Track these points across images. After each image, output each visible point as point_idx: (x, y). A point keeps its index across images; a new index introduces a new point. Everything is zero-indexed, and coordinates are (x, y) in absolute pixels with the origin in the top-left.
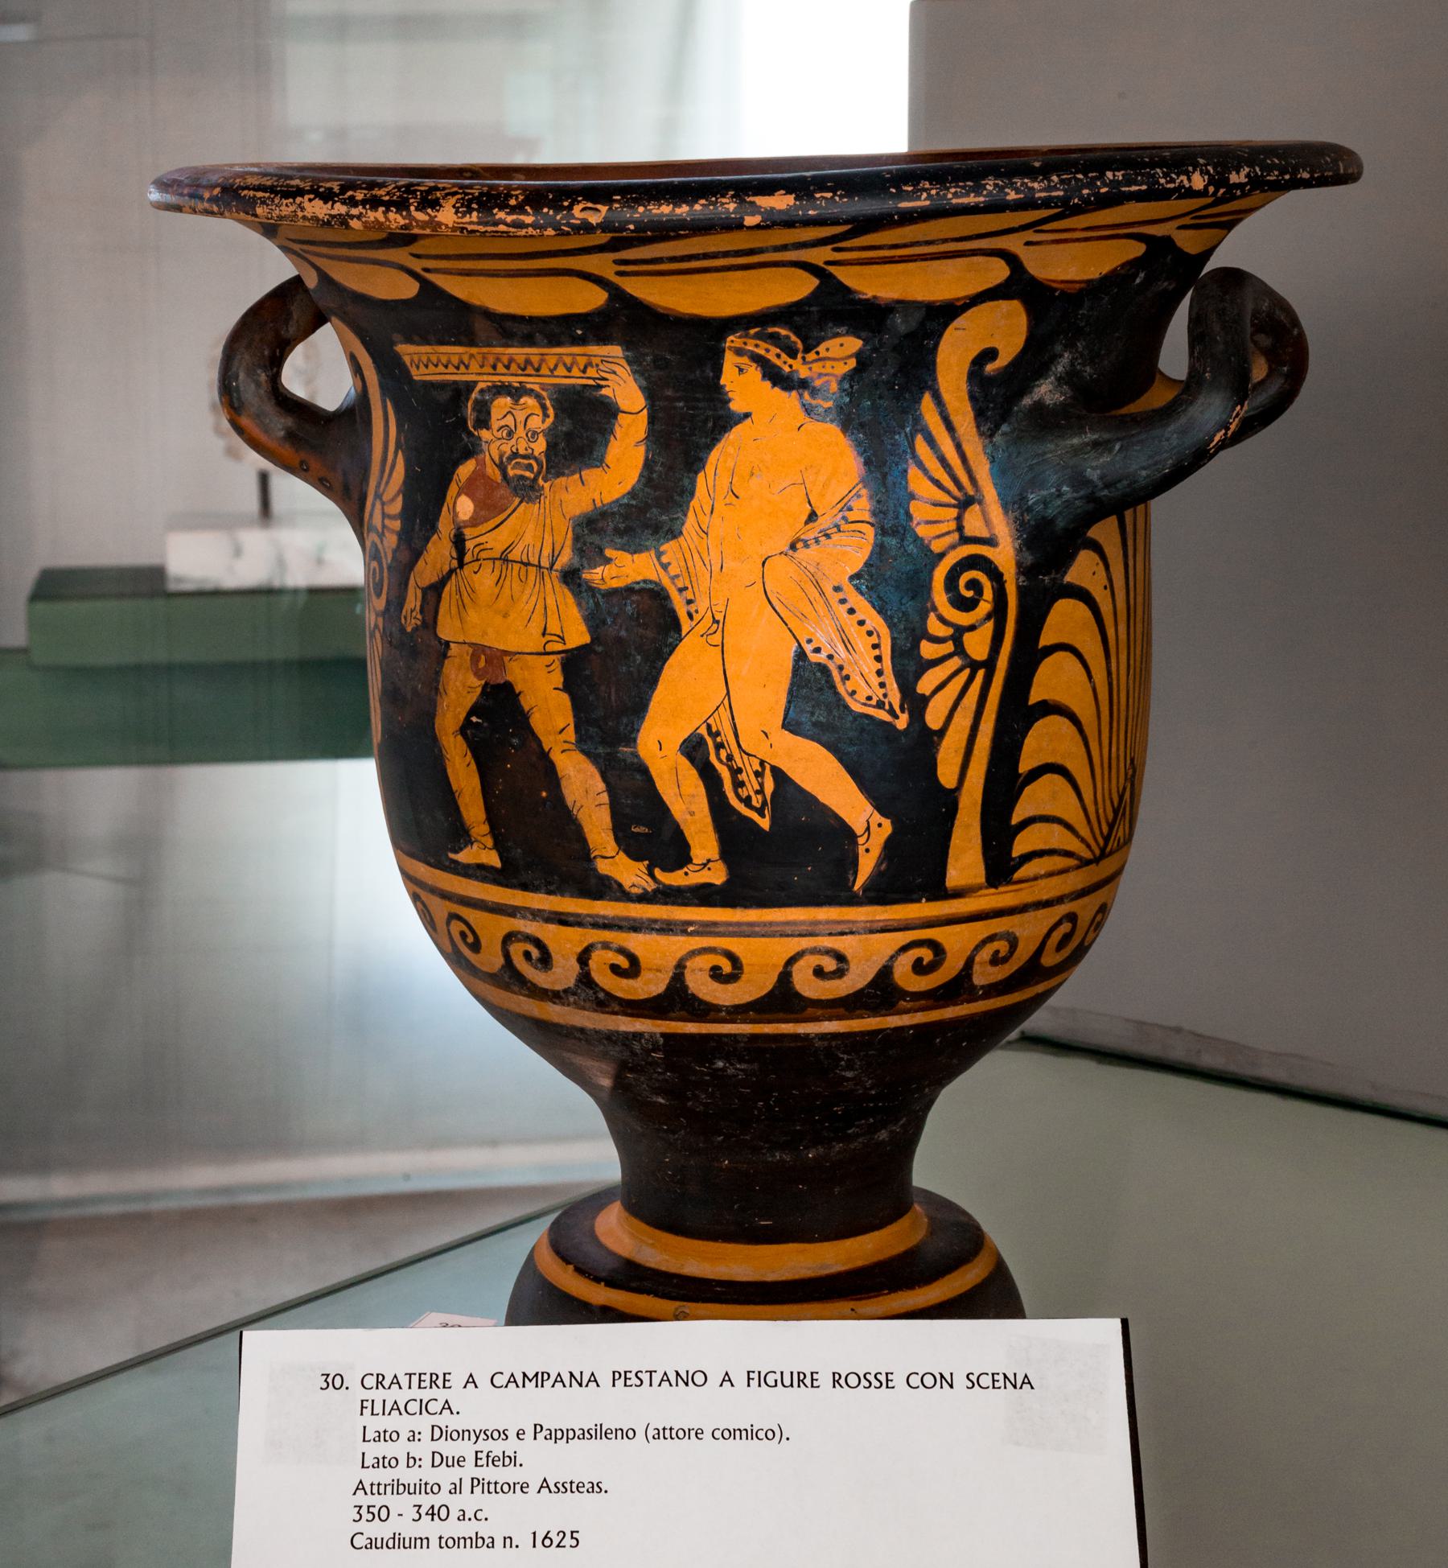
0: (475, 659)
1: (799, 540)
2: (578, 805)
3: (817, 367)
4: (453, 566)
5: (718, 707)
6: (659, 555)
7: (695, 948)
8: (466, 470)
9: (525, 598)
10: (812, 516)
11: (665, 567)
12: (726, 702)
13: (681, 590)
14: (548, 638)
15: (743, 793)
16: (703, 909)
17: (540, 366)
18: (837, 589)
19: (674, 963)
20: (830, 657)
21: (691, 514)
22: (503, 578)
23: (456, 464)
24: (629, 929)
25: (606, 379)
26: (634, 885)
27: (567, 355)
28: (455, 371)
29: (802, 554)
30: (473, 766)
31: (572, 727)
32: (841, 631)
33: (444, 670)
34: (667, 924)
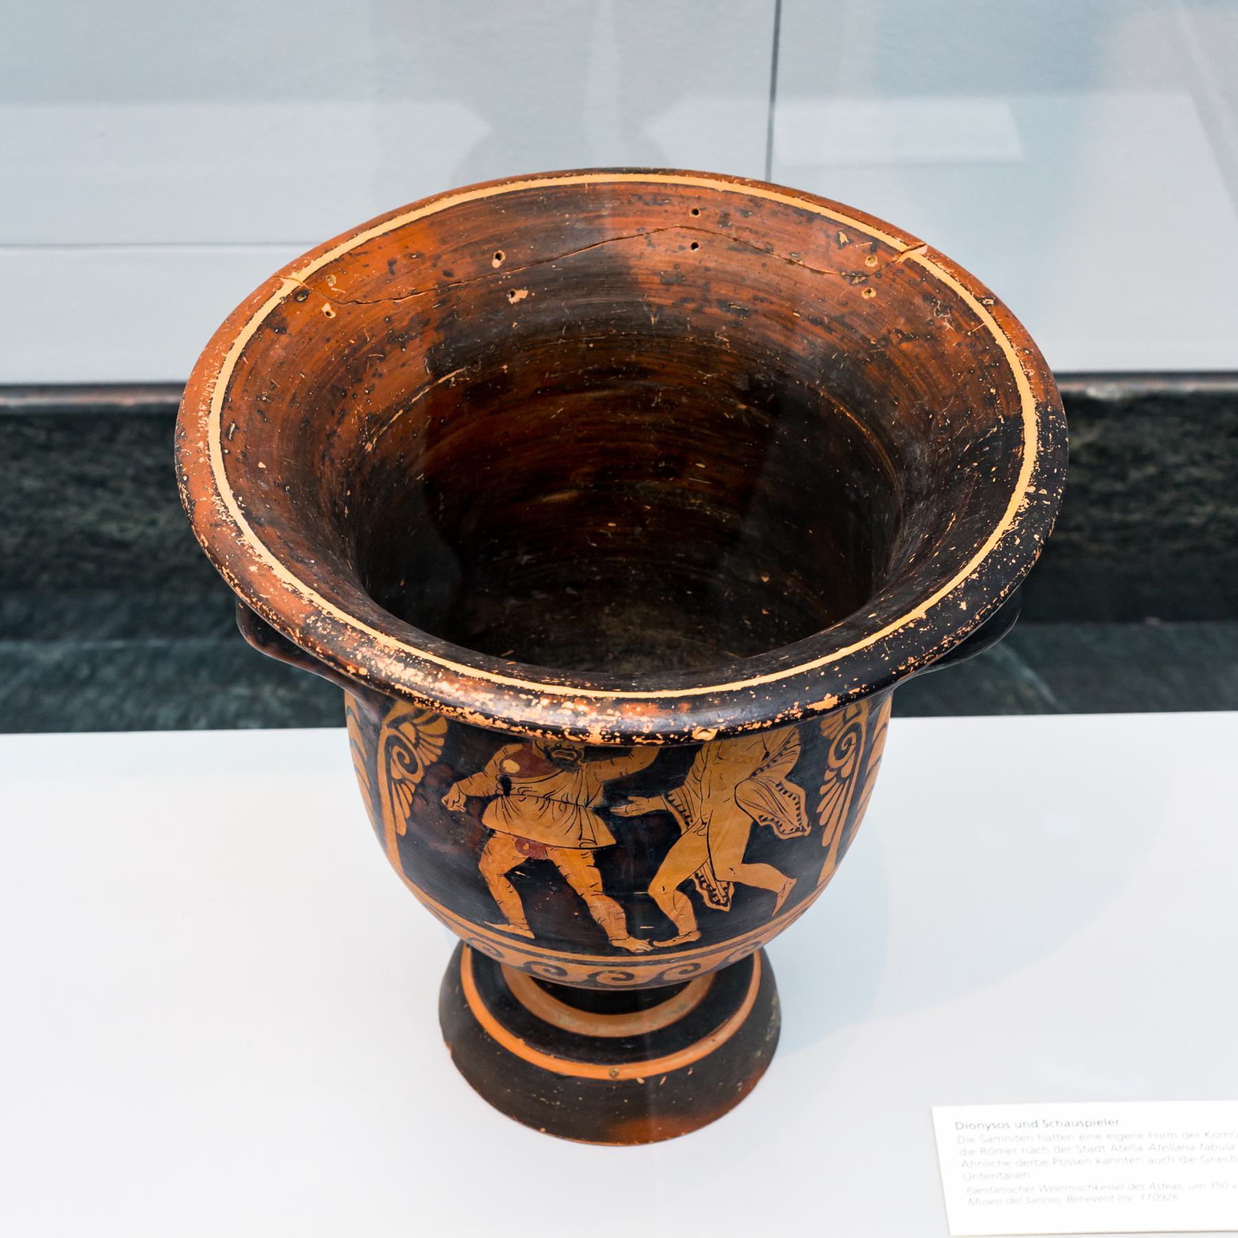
10: (767, 755)
11: (671, 802)
13: (681, 813)
14: (582, 841)
15: (715, 899)
20: (772, 820)
22: (545, 807)
29: (760, 775)
30: (515, 893)
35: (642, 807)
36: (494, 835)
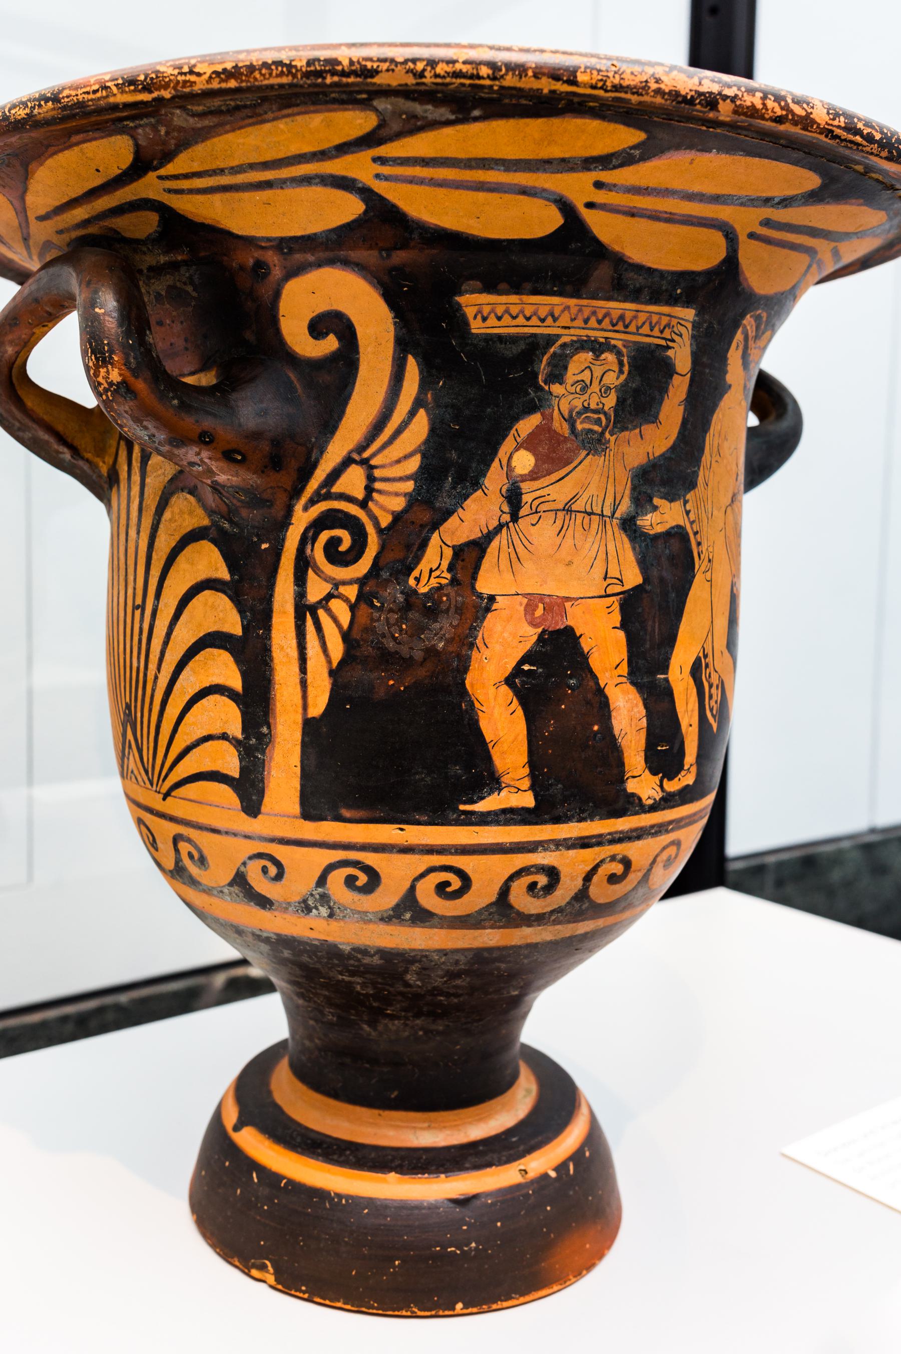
0: (530, 609)
4: (503, 520)
6: (686, 502)
8: (527, 425)
9: (588, 546)
11: (688, 513)
13: (696, 533)
14: (609, 581)
17: (631, 322)
21: (702, 468)
22: (565, 528)
23: (516, 419)
25: (673, 341)
26: (649, 798)
27: (656, 313)
28: (539, 324)
30: (520, 712)
31: (625, 664)
33: (485, 624)
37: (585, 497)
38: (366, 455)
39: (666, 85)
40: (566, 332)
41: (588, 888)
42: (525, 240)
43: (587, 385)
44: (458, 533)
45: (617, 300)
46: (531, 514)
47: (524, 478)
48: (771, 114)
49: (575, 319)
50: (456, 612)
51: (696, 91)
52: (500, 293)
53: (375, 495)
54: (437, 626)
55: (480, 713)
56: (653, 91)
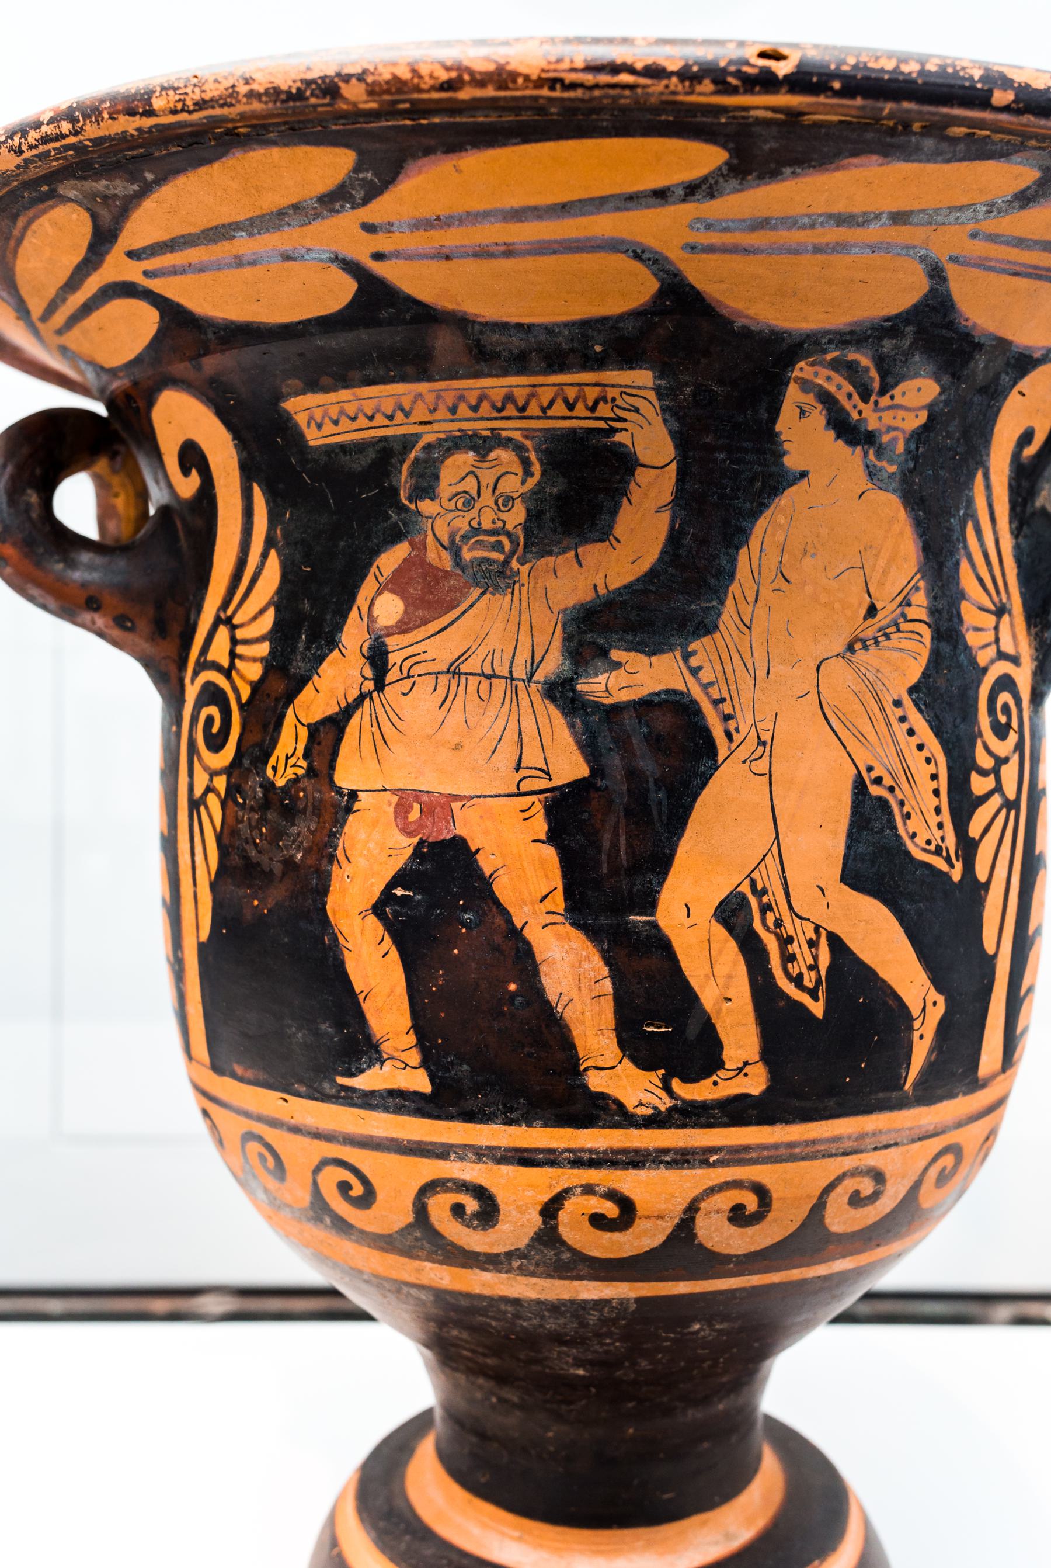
0: (402, 810)
1: (857, 639)
2: (565, 999)
3: (887, 417)
4: (365, 689)
5: (764, 856)
6: (687, 656)
7: (714, 1183)
9: (487, 722)
11: (695, 671)
12: (775, 849)
13: (716, 703)
14: (523, 773)
15: (794, 969)
16: (733, 1129)
18: (897, 703)
19: (685, 1205)
21: (729, 602)
22: (450, 698)
23: (376, 552)
24: (628, 1164)
25: (625, 420)
26: (641, 1104)
27: (572, 385)
28: (387, 422)
29: (860, 656)
30: (394, 954)
32: (901, 755)
33: (346, 829)
34: (683, 1154)
35: (639, 678)
36: (357, 806)
37: (482, 652)
38: (229, 612)
39: (260, 84)
40: (428, 428)
41: (555, 1228)
42: (321, 317)
43: (473, 498)
44: (313, 708)
45: (490, 375)
46: (401, 679)
47: (390, 632)
48: (431, 82)
49: (435, 409)
50: (313, 813)
51: (302, 81)
52: (326, 390)
53: (237, 661)
54: (294, 830)
55: (346, 952)
56: (245, 96)
